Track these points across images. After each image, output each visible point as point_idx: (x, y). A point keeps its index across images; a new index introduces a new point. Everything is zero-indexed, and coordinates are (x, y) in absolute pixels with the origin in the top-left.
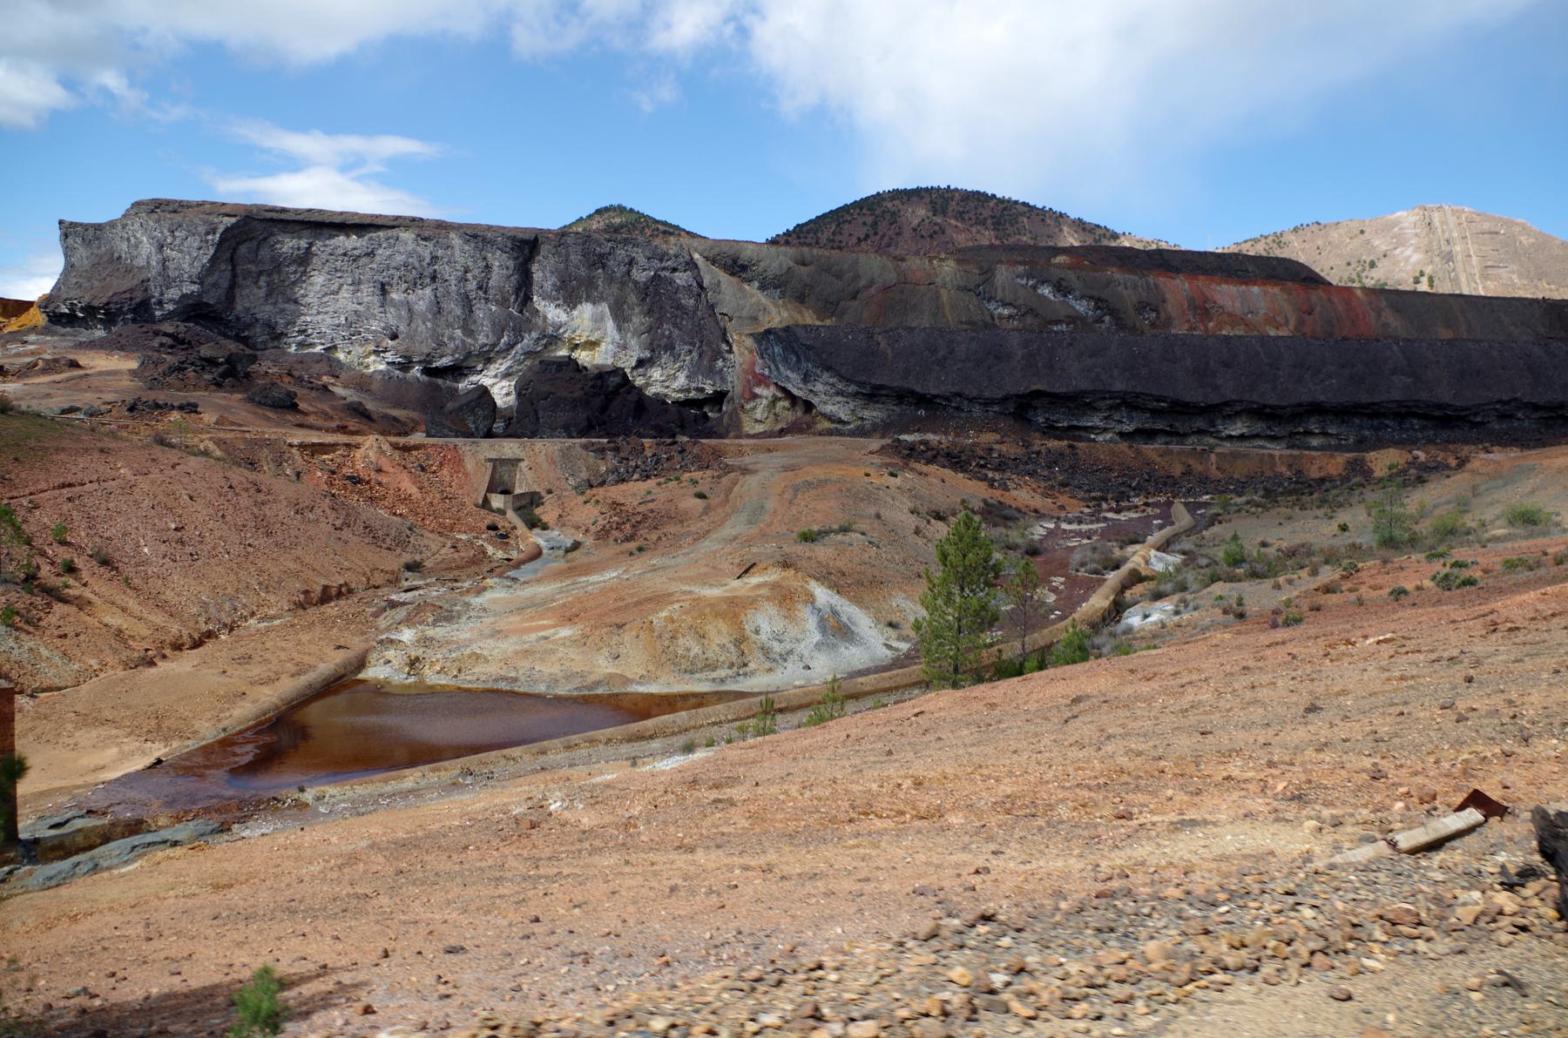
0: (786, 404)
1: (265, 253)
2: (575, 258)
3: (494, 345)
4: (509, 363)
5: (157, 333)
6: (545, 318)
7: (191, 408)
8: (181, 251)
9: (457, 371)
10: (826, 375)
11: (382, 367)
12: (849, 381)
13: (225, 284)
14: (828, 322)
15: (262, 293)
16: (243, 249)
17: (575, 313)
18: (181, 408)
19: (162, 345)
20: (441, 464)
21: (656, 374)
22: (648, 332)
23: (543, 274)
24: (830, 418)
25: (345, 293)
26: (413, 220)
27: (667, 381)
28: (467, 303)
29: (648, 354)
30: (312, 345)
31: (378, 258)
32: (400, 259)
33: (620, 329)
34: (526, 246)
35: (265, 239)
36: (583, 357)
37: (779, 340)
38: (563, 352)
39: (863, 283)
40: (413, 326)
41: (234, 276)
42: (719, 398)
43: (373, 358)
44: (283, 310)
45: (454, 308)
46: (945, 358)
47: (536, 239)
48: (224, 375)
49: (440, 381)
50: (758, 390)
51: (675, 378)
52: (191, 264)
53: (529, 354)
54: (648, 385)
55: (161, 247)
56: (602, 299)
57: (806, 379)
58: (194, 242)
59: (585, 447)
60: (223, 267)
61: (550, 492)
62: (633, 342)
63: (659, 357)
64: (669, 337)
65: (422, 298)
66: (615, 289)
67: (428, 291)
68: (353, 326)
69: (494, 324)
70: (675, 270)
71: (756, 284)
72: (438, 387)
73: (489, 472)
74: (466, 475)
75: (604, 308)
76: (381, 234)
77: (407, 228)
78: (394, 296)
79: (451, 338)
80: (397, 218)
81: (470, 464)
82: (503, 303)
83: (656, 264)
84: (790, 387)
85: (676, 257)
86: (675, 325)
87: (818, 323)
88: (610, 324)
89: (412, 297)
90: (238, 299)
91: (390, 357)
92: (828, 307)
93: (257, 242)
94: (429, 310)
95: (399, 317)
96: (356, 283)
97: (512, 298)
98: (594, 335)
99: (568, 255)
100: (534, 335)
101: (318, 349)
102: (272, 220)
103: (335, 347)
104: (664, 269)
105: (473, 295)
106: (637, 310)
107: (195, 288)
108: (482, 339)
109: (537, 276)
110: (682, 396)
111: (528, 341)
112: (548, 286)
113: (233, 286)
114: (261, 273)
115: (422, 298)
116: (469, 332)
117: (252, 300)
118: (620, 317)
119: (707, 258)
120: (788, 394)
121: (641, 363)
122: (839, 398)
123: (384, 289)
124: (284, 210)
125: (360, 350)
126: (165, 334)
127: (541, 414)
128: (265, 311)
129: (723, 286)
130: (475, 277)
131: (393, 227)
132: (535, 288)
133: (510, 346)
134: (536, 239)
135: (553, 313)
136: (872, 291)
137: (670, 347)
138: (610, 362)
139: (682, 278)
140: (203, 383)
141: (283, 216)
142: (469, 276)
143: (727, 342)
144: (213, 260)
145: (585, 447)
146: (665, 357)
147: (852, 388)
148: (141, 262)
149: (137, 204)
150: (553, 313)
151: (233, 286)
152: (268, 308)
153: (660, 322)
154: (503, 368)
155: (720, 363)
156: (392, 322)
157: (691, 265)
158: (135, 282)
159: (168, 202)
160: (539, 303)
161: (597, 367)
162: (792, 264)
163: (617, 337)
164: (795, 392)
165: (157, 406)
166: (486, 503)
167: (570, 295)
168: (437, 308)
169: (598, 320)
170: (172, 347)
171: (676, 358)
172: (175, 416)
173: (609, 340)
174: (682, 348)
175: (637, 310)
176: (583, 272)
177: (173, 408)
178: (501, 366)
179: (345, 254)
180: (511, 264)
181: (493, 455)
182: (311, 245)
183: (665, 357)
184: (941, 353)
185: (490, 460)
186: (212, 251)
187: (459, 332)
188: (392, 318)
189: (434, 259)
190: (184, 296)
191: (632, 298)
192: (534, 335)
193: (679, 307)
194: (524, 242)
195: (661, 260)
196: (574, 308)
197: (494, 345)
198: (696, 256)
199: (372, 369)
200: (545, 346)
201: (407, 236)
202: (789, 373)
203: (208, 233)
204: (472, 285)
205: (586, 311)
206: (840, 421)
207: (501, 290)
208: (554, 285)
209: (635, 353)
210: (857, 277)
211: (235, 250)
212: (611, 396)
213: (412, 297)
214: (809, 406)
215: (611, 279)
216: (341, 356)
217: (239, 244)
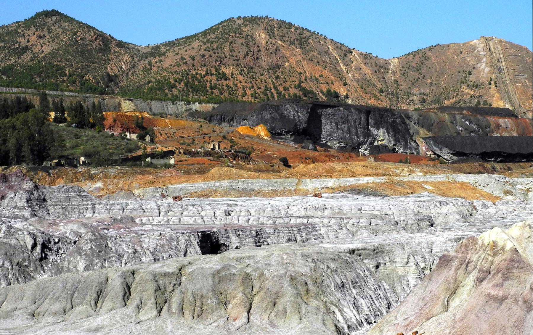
30: (322, 141)
33: (389, 136)
37: (433, 140)
65: (345, 127)
66: (385, 125)
82: (364, 129)
86: (399, 135)
101: (323, 142)
103: (327, 142)
108: (361, 139)
109: (370, 121)
115: (345, 127)
116: (358, 137)
123: (337, 125)
133: (367, 141)
141: (318, 103)
157: (401, 117)
160: (371, 128)
168: (349, 131)
173: (386, 139)
174: (401, 141)
178: (364, 147)
190: (304, 127)
193: (399, 129)
204: (357, 123)
206: (448, 160)
207: (363, 124)
209: (393, 143)
216: (329, 144)
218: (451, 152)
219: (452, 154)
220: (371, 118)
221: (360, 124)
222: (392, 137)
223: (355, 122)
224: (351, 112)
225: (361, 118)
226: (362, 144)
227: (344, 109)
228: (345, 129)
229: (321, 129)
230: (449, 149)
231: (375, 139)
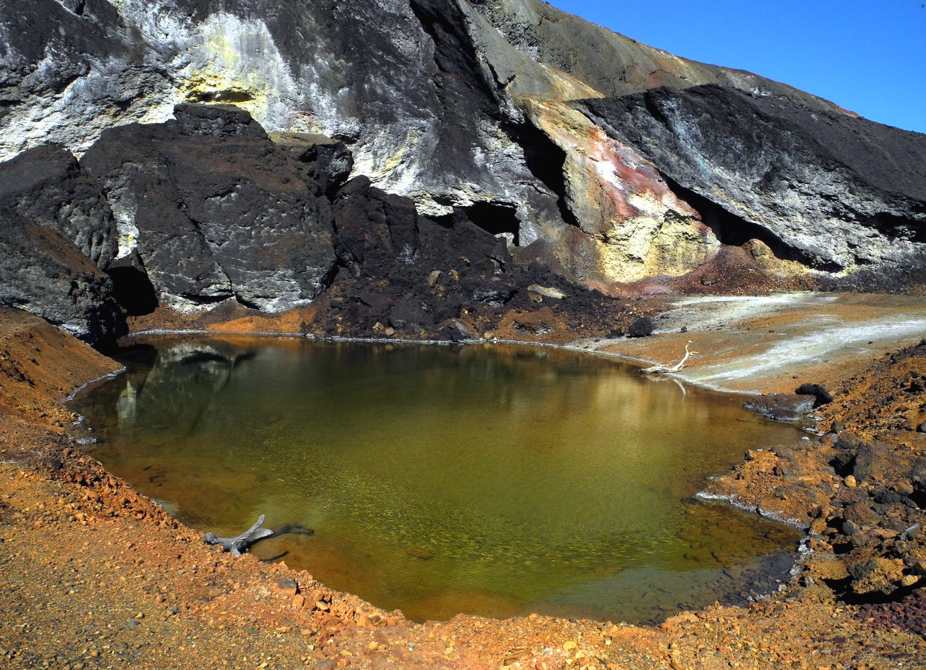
4: (56, 119)
6: (136, 33)
17: (206, 29)
22: (349, 84)
33: (296, 73)
57: (767, 184)
63: (373, 134)
64: (385, 100)
84: (717, 196)
88: (278, 63)
106: (321, 44)
122: (835, 222)
137: (387, 118)
146: (381, 136)
169: (252, 48)
175: (321, 45)
196: (202, 17)
202: (718, 171)
222: (328, 84)
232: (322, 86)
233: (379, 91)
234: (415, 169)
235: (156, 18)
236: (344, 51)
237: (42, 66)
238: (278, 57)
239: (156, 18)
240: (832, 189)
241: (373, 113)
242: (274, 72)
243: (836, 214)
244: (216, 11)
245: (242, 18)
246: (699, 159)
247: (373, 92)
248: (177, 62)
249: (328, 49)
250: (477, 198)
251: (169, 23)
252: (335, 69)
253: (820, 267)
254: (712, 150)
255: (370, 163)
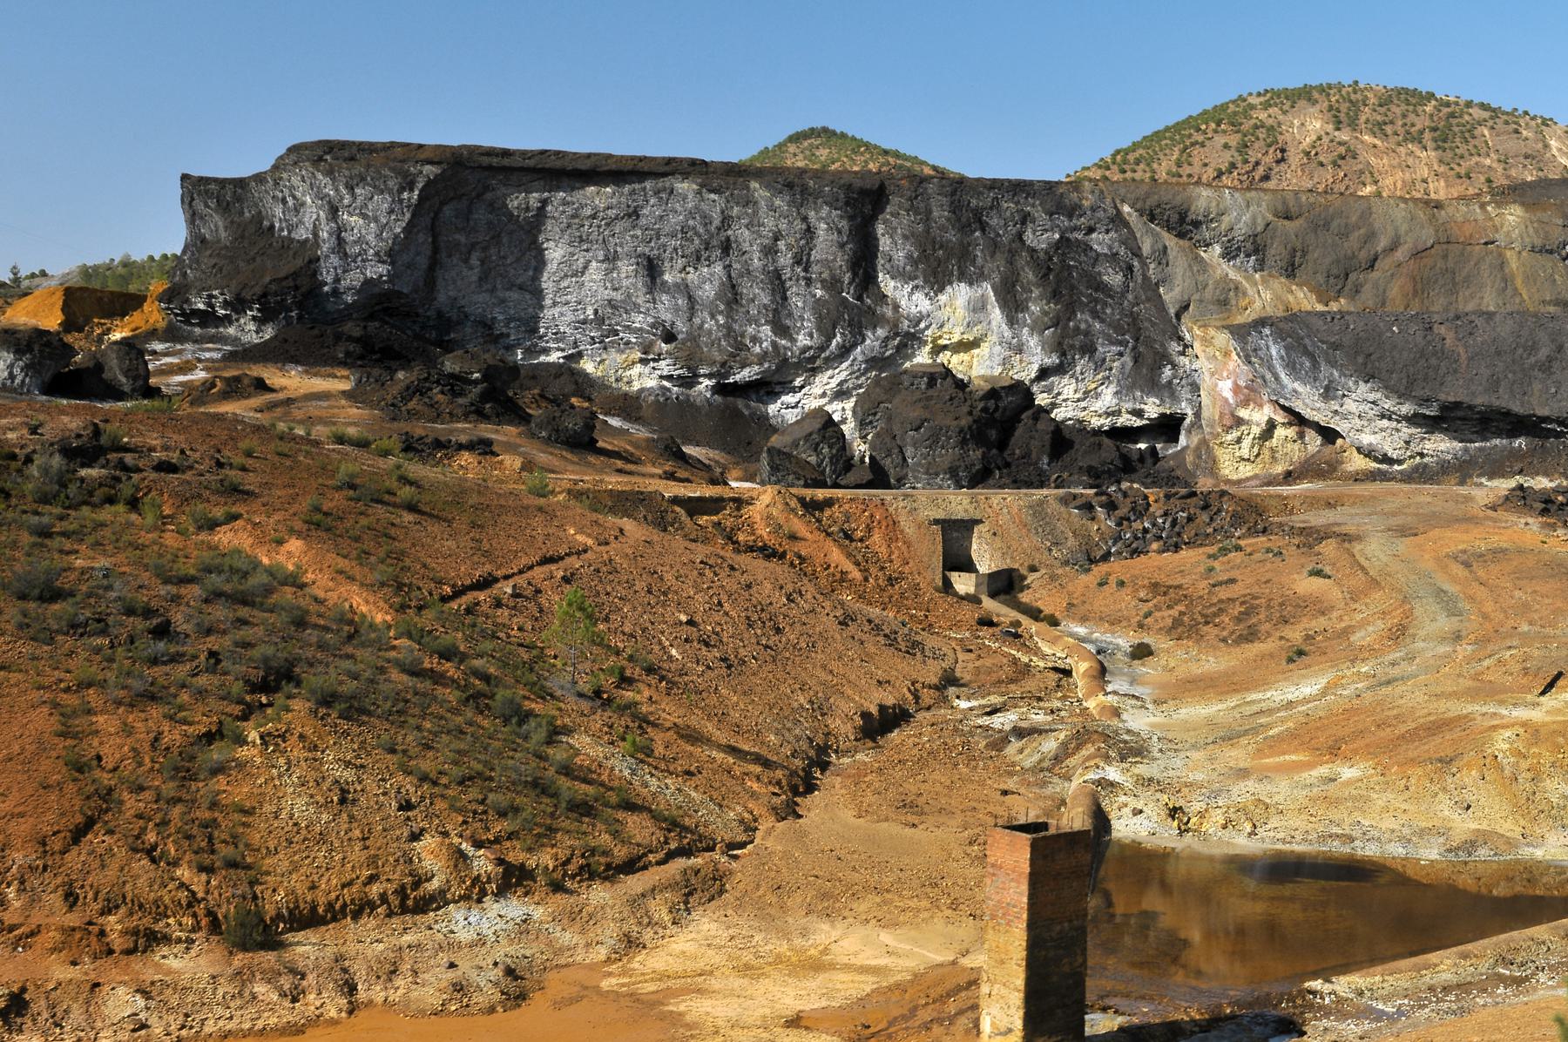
0: (1291, 432)
1: (481, 215)
2: (940, 214)
3: (822, 349)
5: (338, 337)
6: (896, 307)
7: (484, 447)
8: (364, 216)
9: (768, 388)
10: (1363, 387)
11: (651, 383)
12: (1403, 396)
13: (423, 262)
14: (1334, 307)
15: (474, 276)
16: (448, 211)
17: (943, 298)
18: (470, 447)
19: (348, 354)
20: (869, 529)
21: (1067, 387)
22: (1056, 325)
23: (892, 243)
24: (1368, 453)
25: (595, 272)
26: (693, 163)
27: (1087, 400)
28: (777, 284)
29: (1054, 360)
30: (546, 351)
31: (643, 221)
32: (675, 220)
33: (1012, 322)
34: (865, 201)
35: (479, 196)
36: (956, 363)
38: (922, 358)
39: (1383, 243)
40: (697, 321)
41: (436, 250)
42: (1169, 427)
43: (638, 368)
44: (503, 301)
45: (757, 294)
46: (1550, 359)
47: (882, 187)
48: (485, 397)
49: (740, 403)
50: (1243, 413)
51: (1097, 396)
52: (379, 236)
53: (874, 362)
54: (1054, 405)
55: (334, 211)
56: (981, 276)
57: (1328, 393)
58: (381, 203)
59: (1065, 501)
60: (421, 237)
61: (1033, 569)
62: (1033, 342)
63: (1073, 363)
64: (1087, 333)
65: (707, 280)
66: (1000, 262)
67: (718, 268)
68: (605, 328)
69: (820, 318)
70: (1091, 230)
71: (1217, 249)
72: (737, 413)
73: (939, 538)
74: (908, 544)
75: (987, 289)
76: (648, 184)
77: (686, 175)
78: (667, 277)
79: (755, 339)
80: (669, 161)
81: (907, 527)
82: (833, 285)
83: (1064, 221)
84: (1299, 407)
85: (1093, 210)
86: (1096, 315)
87: (1320, 308)
88: (996, 315)
89: (692, 277)
90: (440, 283)
91: (665, 367)
92: (1340, 278)
93: (474, 202)
94: (718, 296)
95: (677, 310)
96: (611, 259)
97: (847, 278)
98: (972, 334)
99: (929, 212)
100: (881, 332)
101: (554, 357)
102: (490, 168)
103: (580, 355)
104: (1076, 228)
105: (787, 273)
106: (1036, 293)
107: (382, 269)
108: (803, 340)
109: (885, 243)
110: (1106, 423)
111: (872, 341)
112: (900, 256)
113: (434, 264)
114: (473, 246)
115: (707, 280)
116: (782, 330)
117: (461, 286)
118: (1012, 304)
119: (1141, 212)
120: (1298, 420)
121: (1044, 373)
122: (1385, 423)
123: (652, 269)
124: (506, 153)
125: (620, 358)
126: (350, 339)
127: (909, 451)
128: (478, 302)
129: (1172, 254)
130: (789, 247)
131: (665, 175)
132: (881, 261)
133: (845, 351)
134: (882, 187)
135: (909, 299)
136: (1400, 254)
137: (1089, 349)
138: (997, 371)
139: (1101, 241)
140: (459, 411)
141: (506, 162)
142: (781, 244)
143: (1181, 339)
144: (408, 229)
145: (1065, 501)
146: (1081, 364)
147: (1407, 409)
148: (302, 234)
149: (292, 150)
150: (909, 299)
151: (434, 264)
152: (481, 298)
153: (1071, 309)
154: (834, 383)
155: (1167, 372)
156: (667, 317)
157: (1118, 220)
158: (299, 262)
159: (343, 145)
160: (888, 284)
161: (984, 378)
162: (1270, 217)
163: (1008, 334)
164: (1307, 413)
165: (439, 444)
166: (947, 586)
167: (936, 271)
168: (732, 296)
169: (978, 307)
170: (362, 357)
171: (1100, 365)
172: (466, 458)
173: (993, 338)
174: (1105, 349)
176: (952, 236)
177: (461, 447)
179: (594, 217)
180: (844, 224)
181: (941, 515)
182: (544, 202)
183: (1081, 364)
184: (1543, 353)
185: (936, 522)
186: (408, 216)
187: (766, 330)
188: (666, 309)
189: (726, 221)
191: (1029, 275)
192: (881, 332)
193: (1101, 287)
194: (863, 192)
195: (1070, 217)
196: (941, 290)
197: (822, 349)
198: (1126, 209)
199: (636, 386)
200: (898, 348)
201: (685, 187)
202: (1297, 385)
203: (401, 190)
204: (785, 259)
205: (959, 296)
207: (826, 263)
208: (909, 257)
209: (1036, 357)
210: (1371, 236)
211: (436, 214)
212: (1007, 426)
213: (692, 277)
214: (1329, 435)
215: (994, 246)
216: (588, 366)
217: (443, 204)
218: (1407, 409)
219: (1412, 420)
220: (891, 232)
221: (802, 260)
222: (1038, 328)
223: (770, 251)
224: (749, 202)
225: (809, 232)
226: (811, 365)
227: (702, 186)
228: (708, 291)
229: (538, 294)
230: (1390, 390)
231: (910, 340)
232: (1032, 329)
233: (1083, 326)
234: (1112, 388)
235: (911, 294)
236: (1055, 295)
237: (834, 342)
238: (997, 311)
239: (911, 294)
240: (1372, 397)
241: (1072, 347)
242: (994, 323)
243: (1383, 416)
244: (951, 283)
245: (971, 284)
246: (1283, 376)
247: (1077, 329)
248: (922, 325)
249: (1041, 297)
250: (1161, 410)
251: (919, 297)
252: (1045, 313)
253: (1381, 462)
254: (1292, 367)
255: (1073, 386)
